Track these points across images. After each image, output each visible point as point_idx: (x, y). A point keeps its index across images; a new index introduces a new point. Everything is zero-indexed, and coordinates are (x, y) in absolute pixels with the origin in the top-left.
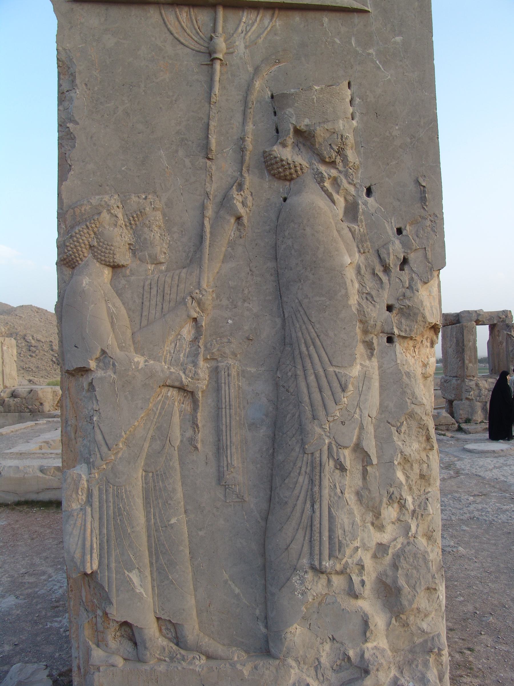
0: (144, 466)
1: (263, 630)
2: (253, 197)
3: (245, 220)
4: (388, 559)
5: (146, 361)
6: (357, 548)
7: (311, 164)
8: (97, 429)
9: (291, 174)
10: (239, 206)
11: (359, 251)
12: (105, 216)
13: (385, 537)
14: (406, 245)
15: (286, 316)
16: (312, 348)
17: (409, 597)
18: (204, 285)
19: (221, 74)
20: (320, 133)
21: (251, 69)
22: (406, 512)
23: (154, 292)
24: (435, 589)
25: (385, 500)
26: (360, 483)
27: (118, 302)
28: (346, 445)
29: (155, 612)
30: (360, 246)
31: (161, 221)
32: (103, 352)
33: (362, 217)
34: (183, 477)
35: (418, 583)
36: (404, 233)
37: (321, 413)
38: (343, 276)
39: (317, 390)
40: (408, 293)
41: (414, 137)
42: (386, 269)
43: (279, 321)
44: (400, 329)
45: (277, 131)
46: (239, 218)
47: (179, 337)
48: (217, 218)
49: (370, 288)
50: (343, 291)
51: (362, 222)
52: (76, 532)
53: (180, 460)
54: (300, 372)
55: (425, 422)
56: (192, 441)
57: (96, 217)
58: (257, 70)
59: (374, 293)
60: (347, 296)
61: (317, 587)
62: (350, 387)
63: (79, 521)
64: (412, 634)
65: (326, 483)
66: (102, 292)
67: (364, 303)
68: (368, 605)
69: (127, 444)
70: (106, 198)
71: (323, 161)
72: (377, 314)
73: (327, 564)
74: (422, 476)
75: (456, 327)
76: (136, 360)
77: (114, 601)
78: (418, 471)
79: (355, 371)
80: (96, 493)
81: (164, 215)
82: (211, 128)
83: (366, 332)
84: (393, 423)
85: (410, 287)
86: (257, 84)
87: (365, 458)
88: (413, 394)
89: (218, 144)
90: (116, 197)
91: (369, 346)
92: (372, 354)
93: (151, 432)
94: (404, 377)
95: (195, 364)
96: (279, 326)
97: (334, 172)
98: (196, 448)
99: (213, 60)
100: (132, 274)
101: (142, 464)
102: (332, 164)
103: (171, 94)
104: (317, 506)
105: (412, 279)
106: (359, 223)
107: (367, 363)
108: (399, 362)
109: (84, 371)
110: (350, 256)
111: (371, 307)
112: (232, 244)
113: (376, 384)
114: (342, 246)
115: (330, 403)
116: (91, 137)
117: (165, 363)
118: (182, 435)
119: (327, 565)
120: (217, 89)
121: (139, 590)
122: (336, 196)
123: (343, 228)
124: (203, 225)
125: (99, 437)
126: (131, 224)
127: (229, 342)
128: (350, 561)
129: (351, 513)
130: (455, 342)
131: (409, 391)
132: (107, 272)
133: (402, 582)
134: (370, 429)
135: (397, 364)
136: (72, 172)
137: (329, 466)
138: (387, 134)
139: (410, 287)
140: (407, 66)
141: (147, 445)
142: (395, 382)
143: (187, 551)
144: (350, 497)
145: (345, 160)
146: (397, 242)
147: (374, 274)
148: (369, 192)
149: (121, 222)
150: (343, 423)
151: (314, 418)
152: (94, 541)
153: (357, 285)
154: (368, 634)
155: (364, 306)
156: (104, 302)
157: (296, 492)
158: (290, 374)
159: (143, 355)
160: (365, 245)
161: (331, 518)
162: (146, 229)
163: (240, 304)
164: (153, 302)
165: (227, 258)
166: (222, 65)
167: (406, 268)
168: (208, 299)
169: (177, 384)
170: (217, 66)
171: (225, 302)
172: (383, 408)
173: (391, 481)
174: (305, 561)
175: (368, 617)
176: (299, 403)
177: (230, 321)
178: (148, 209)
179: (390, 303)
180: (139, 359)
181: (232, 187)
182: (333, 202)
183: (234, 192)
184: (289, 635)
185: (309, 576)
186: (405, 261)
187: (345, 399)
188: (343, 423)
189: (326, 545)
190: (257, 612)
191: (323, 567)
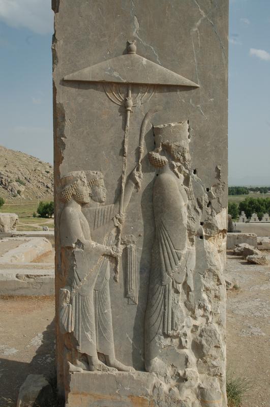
1: (143, 359)
2: (143, 179)
4: (198, 332)
6: (183, 326)
8: (75, 272)
9: (160, 164)
10: (137, 178)
11: (189, 199)
12: (79, 181)
13: (197, 323)
14: (210, 196)
15: (156, 226)
16: (166, 241)
17: (207, 349)
19: (130, 116)
21: (144, 115)
23: (100, 215)
24: (220, 347)
25: (197, 306)
26: (186, 298)
27: (85, 219)
28: (180, 282)
32: (78, 240)
34: (111, 293)
36: (210, 191)
37: (169, 268)
39: (168, 259)
40: (210, 217)
41: (217, 147)
42: (201, 207)
43: (153, 228)
44: (206, 233)
45: (155, 143)
46: (137, 184)
47: (110, 234)
50: (180, 218)
51: (191, 186)
52: (65, 315)
53: (110, 285)
54: (161, 251)
56: (115, 279)
57: (75, 182)
58: (146, 115)
60: (182, 220)
61: (166, 342)
62: (182, 258)
63: (67, 311)
64: (209, 366)
65: (171, 298)
67: (190, 221)
68: (188, 352)
69: (88, 279)
70: (80, 172)
72: (196, 226)
73: (170, 332)
74: (216, 297)
76: (92, 244)
77: (80, 344)
79: (184, 252)
80: (74, 299)
81: (105, 181)
82: (126, 142)
83: (190, 234)
85: (211, 215)
86: (146, 122)
87: (187, 288)
88: (211, 261)
89: (129, 149)
90: (84, 172)
91: (192, 240)
92: (193, 244)
93: (98, 274)
94: (207, 254)
95: (117, 245)
96: (153, 230)
97: (179, 164)
98: (116, 281)
99: (127, 111)
100: (91, 206)
102: (179, 160)
103: (108, 125)
104: (166, 307)
105: (212, 211)
107: (191, 247)
108: (205, 247)
109: (71, 248)
110: (184, 201)
112: (133, 194)
113: (194, 257)
115: (173, 264)
116: (72, 145)
118: (111, 275)
121: (90, 340)
122: (179, 173)
124: (121, 186)
125: (76, 276)
127: (132, 236)
129: (181, 311)
132: (79, 206)
133: (204, 342)
134: (191, 276)
135: (204, 248)
136: (64, 160)
137: (172, 291)
138: (204, 145)
139: (211, 215)
141: (96, 279)
142: (202, 256)
143: (112, 324)
144: (181, 304)
146: (206, 195)
147: (195, 209)
148: (195, 172)
149: (86, 184)
150: (179, 273)
151: (167, 270)
152: (72, 319)
153: (187, 214)
154: (188, 364)
157: (158, 301)
158: (157, 252)
161: (173, 313)
162: (97, 187)
163: (136, 220)
164: (100, 219)
165: (132, 200)
166: (131, 112)
167: (210, 206)
168: (123, 218)
169: (109, 254)
170: (129, 113)
171: (130, 219)
172: (197, 267)
173: (199, 298)
174: (161, 330)
175: (188, 357)
176: (160, 264)
179: (202, 221)
180: (93, 243)
181: (134, 169)
182: (178, 177)
183: (135, 172)
184: (153, 362)
185: (162, 337)
188: (179, 273)
189: (170, 324)
190: (140, 352)
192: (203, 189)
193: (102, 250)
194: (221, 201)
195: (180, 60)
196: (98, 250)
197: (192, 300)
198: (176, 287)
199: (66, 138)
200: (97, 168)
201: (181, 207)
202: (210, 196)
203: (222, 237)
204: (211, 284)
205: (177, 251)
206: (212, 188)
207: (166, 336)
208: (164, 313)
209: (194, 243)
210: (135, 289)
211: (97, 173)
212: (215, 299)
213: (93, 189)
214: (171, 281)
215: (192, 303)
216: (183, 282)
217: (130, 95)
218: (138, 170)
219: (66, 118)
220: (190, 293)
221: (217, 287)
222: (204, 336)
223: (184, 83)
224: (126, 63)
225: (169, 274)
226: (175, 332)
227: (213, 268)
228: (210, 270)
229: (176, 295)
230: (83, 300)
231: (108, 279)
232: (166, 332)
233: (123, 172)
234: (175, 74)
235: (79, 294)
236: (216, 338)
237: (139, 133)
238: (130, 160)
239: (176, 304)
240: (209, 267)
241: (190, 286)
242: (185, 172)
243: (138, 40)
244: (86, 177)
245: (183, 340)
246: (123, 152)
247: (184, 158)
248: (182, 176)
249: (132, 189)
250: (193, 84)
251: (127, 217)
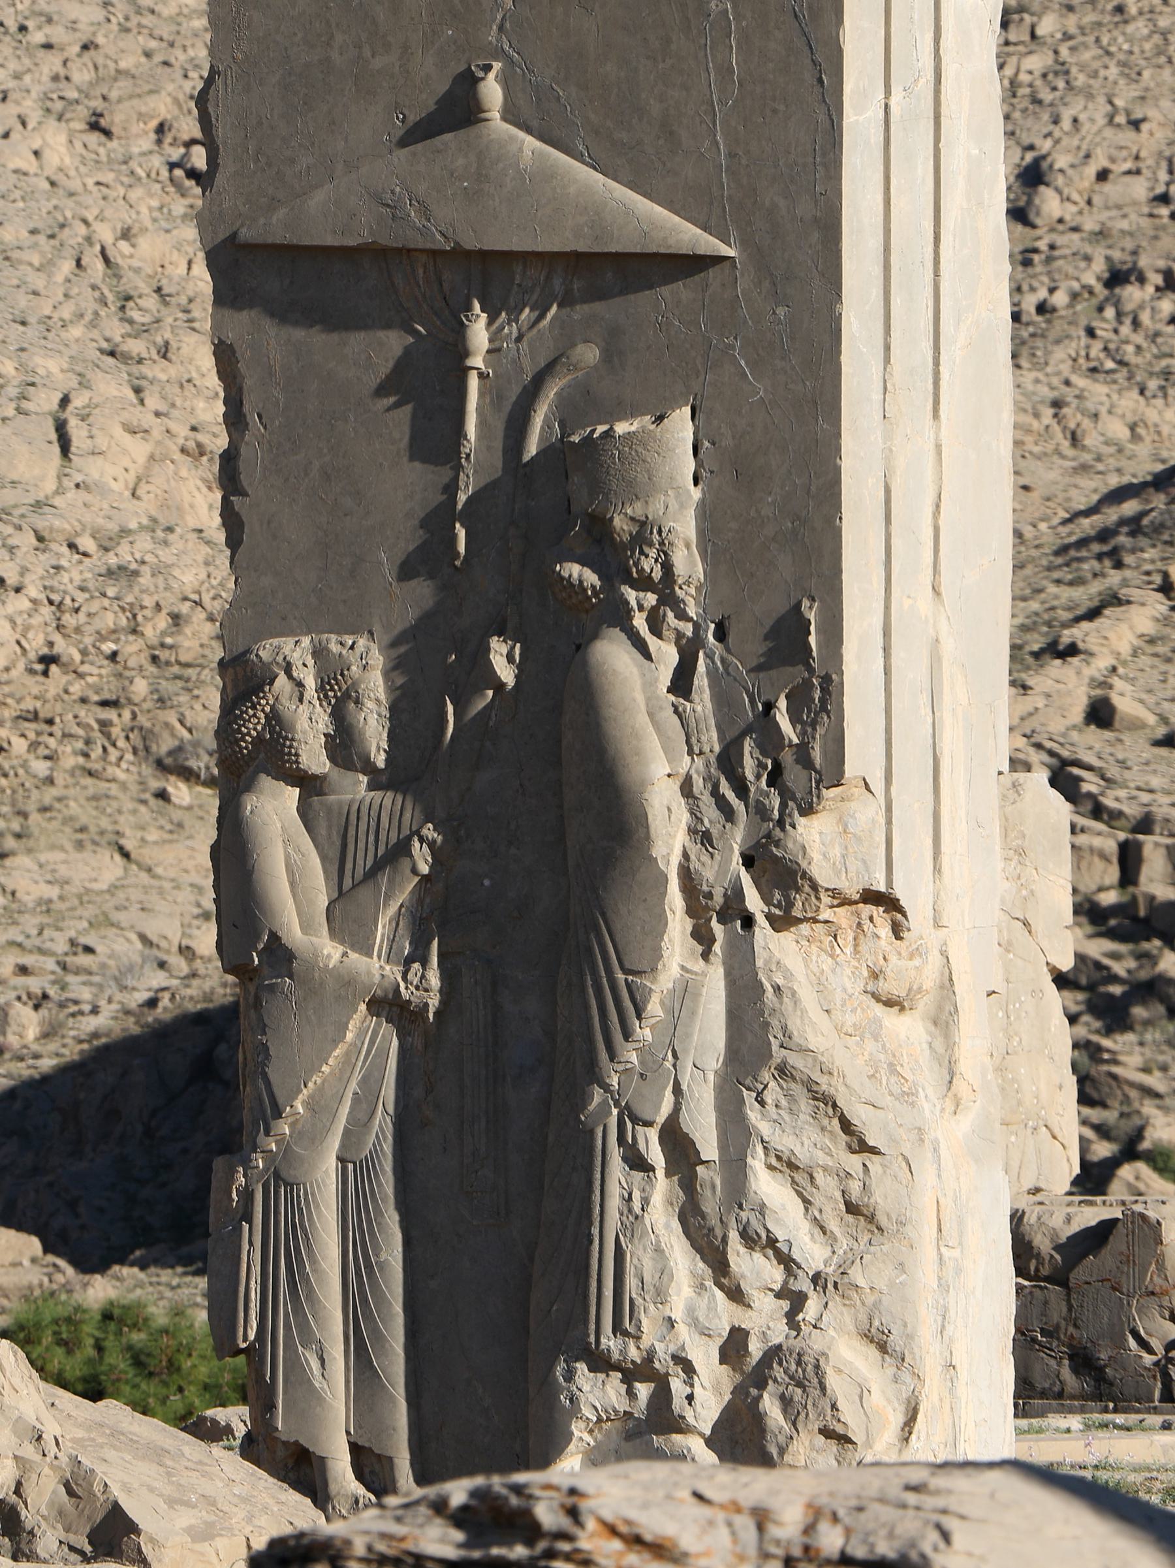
0: (340, 1149)
5: (345, 954)
11: (690, 752)
17: (781, 1439)
19: (481, 394)
22: (800, 1272)
24: (849, 1441)
25: (734, 1236)
28: (647, 1117)
29: (348, 1433)
30: (694, 740)
31: (381, 689)
32: (274, 937)
33: (706, 682)
35: (803, 1415)
40: (777, 832)
49: (711, 822)
55: (824, 1087)
59: (715, 832)
62: (654, 1008)
66: (279, 825)
67: (694, 850)
69: (309, 1104)
73: (610, 1343)
78: (838, 1195)
84: (748, 1082)
88: (784, 1029)
93: (353, 1086)
97: (651, 599)
101: (337, 1145)
102: (643, 583)
105: (783, 806)
106: (695, 696)
107: (699, 965)
108: (759, 963)
111: (705, 858)
114: (652, 743)
115: (618, 1036)
117: (379, 958)
119: (611, 1343)
122: (652, 642)
123: (661, 708)
126: (326, 696)
128: (660, 1347)
131: (774, 1022)
140: (793, 368)
147: (715, 793)
148: (721, 635)
153: (685, 817)
155: (693, 857)
156: (280, 844)
159: (342, 943)
160: (704, 738)
166: (481, 375)
170: (473, 383)
177: (487, 882)
178: (354, 668)
180: (331, 951)
182: (648, 656)
185: (581, 1367)
187: (647, 1031)
191: (603, 1347)
193: (364, 978)
194: (817, 755)
195: (661, 142)
196: (348, 983)
198: (634, 1137)
200: (352, 623)
201: (644, 783)
203: (885, 931)
204: (810, 1142)
205: (630, 978)
206: (782, 703)
207: (601, 1363)
209: (717, 948)
211: (352, 648)
212: (850, 1218)
214: (615, 1112)
216: (661, 1119)
219: (246, 408)
220: (700, 1169)
221: (854, 1163)
222: (775, 1381)
223: (671, 241)
224: (461, 161)
226: (631, 1343)
227: (794, 1060)
228: (783, 1071)
229: (638, 1176)
230: (290, 1202)
232: (592, 1339)
236: (823, 1388)
239: (633, 1219)
240: (778, 1054)
241: (696, 1136)
242: (679, 635)
244: (310, 662)
245: (677, 1386)
247: (667, 567)
248: (667, 655)
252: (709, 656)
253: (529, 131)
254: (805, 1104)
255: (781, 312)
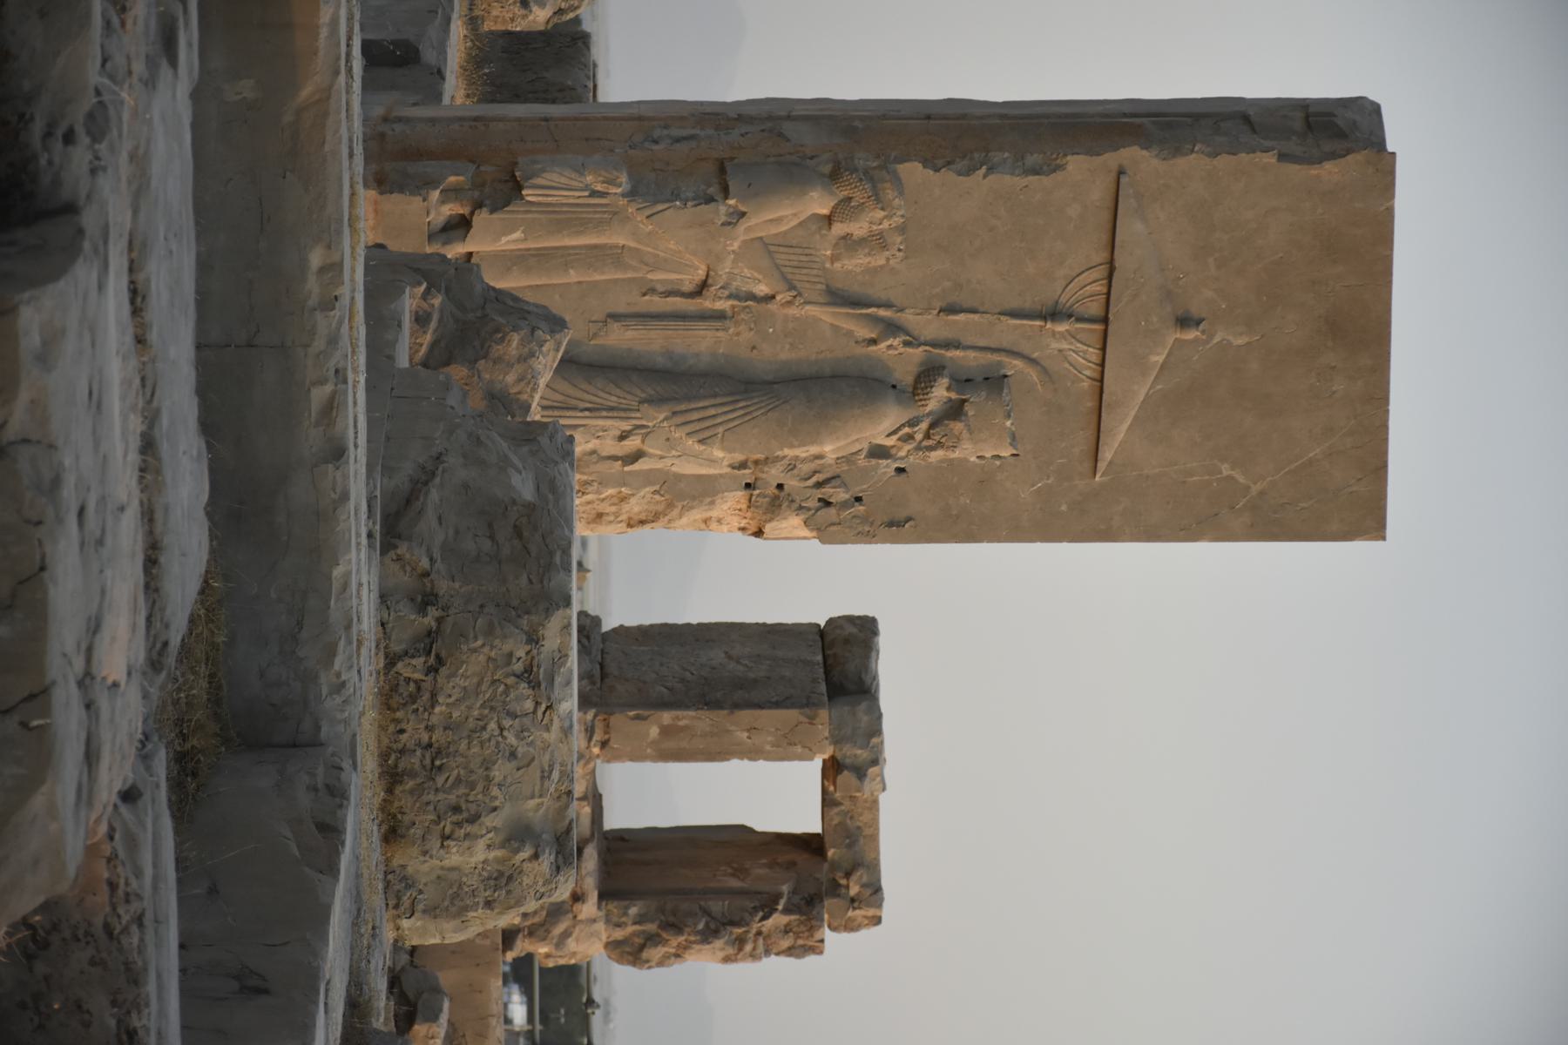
3: (873, 348)
7: (929, 414)
14: (845, 505)
18: (808, 307)
20: (958, 426)
21: (1035, 355)
32: (743, 214)
34: (616, 281)
37: (679, 419)
38: (812, 443)
46: (874, 342)
48: (876, 320)
52: (563, 180)
53: (634, 279)
54: (719, 400)
56: (652, 291)
60: (792, 446)
65: (609, 423)
67: (786, 462)
71: (932, 426)
72: (774, 474)
74: (600, 516)
75: (815, 681)
77: (495, 216)
79: (718, 453)
81: (882, 267)
83: (756, 462)
85: (801, 508)
86: (1018, 363)
91: (743, 465)
95: (730, 297)
97: (919, 437)
102: (927, 436)
105: (809, 509)
107: (726, 463)
109: (726, 192)
112: (850, 333)
113: (704, 471)
114: (842, 443)
115: (689, 428)
120: (1018, 322)
121: (504, 239)
122: (895, 437)
125: (660, 207)
130: (751, 675)
134: (659, 465)
137: (625, 426)
139: (801, 508)
145: (931, 448)
146: (847, 496)
147: (815, 472)
148: (900, 470)
151: (674, 413)
152: (557, 197)
165: (835, 328)
168: (793, 311)
170: (1038, 323)
171: (791, 325)
172: (679, 477)
176: (689, 399)
186: (828, 504)
192: (857, 490)
197: (604, 467)
199: (985, 177)
202: (845, 505)
204: (635, 506)
208: (574, 408)
210: (621, 338)
213: (862, 241)
215: (593, 468)
217: (1079, 325)
218: (906, 344)
219: (1030, 178)
221: (624, 517)
225: (666, 419)
227: (676, 512)
228: (670, 505)
229: (618, 433)
231: (650, 276)
233: (902, 310)
234: (1125, 426)
235: (615, 213)
237: (993, 345)
238: (930, 326)
240: (679, 505)
242: (900, 449)
243: (1207, 342)
246: (951, 309)
249: (865, 332)
250: (1102, 466)
251: (796, 319)
252: (887, 466)
253: (1169, 355)
254: (653, 508)
255: (1064, 508)
